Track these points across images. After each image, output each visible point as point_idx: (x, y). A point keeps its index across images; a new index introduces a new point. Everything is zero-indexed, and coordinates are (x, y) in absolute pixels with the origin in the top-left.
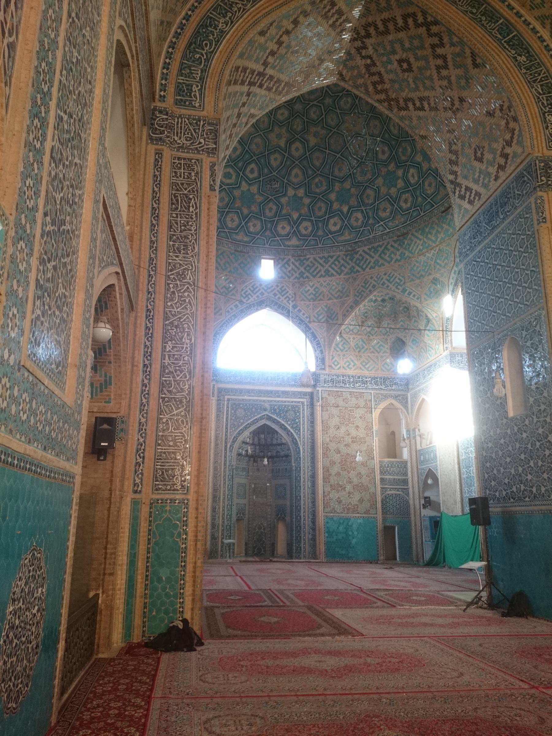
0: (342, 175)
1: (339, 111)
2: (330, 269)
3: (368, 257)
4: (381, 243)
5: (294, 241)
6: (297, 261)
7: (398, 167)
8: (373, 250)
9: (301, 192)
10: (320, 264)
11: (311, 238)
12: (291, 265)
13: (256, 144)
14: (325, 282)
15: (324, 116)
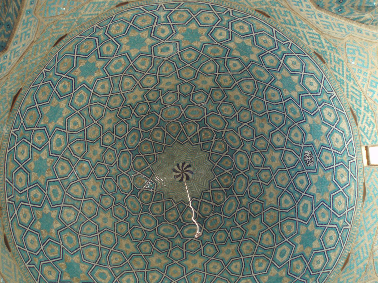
0: (276, 92)
1: (237, 113)
2: (345, 75)
3: (308, 37)
4: (288, 30)
5: (343, 125)
6: (359, 118)
7: (231, 50)
8: (299, 35)
9: (306, 127)
10: (347, 88)
11: (333, 106)
12: (363, 124)
13: (282, 181)
14: (359, 77)
15: (246, 124)
